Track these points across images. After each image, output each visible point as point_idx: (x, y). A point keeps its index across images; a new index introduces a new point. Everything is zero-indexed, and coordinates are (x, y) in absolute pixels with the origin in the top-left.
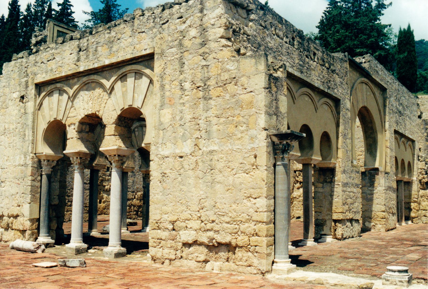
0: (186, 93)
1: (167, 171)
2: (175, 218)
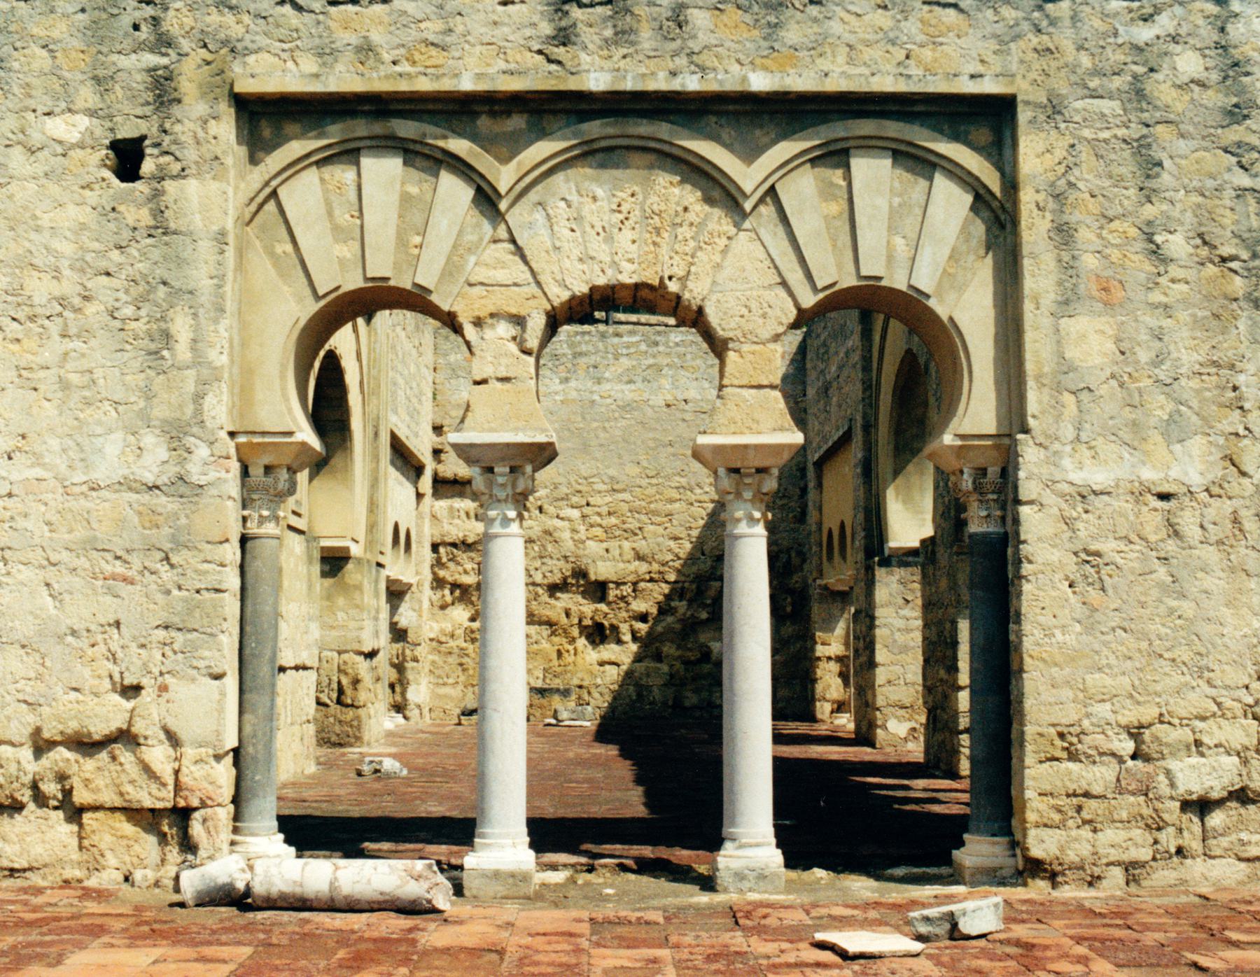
0: (1174, 271)
1: (1108, 546)
2: (1148, 713)
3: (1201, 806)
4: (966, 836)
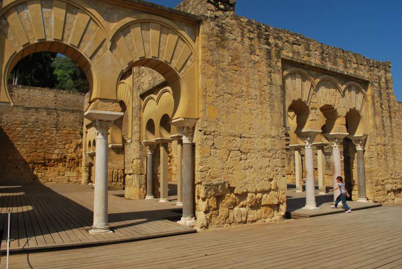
1: (380, 153)
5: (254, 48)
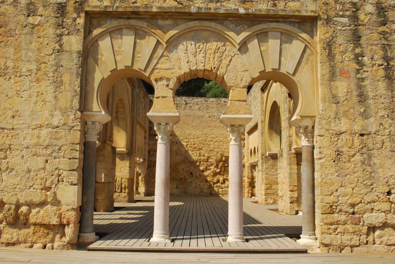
0: (365, 69)
3: (372, 229)
4: (301, 236)
5: (35, 7)
